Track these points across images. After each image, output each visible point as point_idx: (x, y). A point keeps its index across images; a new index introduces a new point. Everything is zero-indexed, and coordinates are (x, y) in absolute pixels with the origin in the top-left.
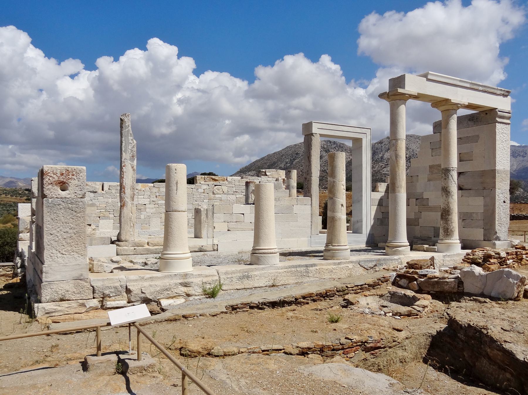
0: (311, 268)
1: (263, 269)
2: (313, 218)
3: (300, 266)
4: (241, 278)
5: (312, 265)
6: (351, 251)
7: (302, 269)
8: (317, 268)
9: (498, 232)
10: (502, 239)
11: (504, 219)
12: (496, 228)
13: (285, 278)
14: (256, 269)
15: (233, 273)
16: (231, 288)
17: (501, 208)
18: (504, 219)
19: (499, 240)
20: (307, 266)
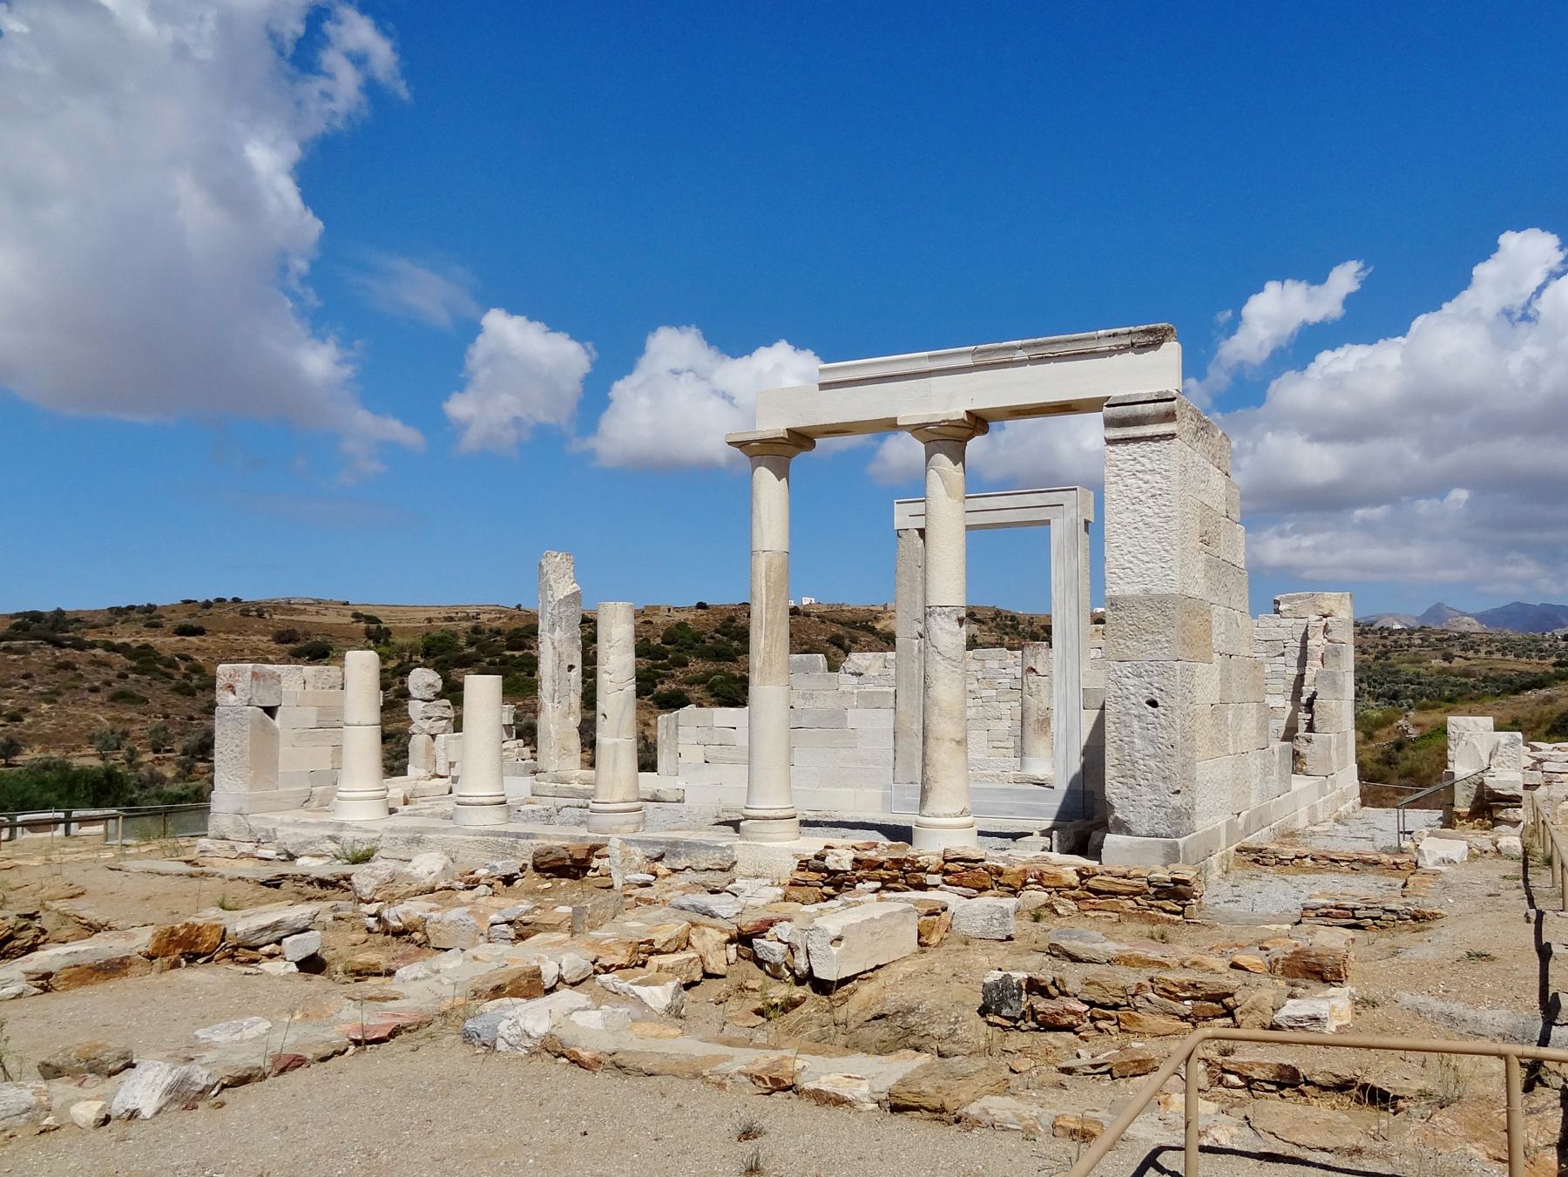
0: (522, 841)
1: (445, 831)
2: (900, 742)
3: (506, 834)
4: (409, 842)
5: (528, 836)
6: (981, 833)
7: (506, 840)
8: (534, 842)
9: (1116, 802)
10: (1133, 828)
11: (1152, 763)
12: (1108, 791)
13: (473, 853)
14: (435, 830)
15: (401, 831)
16: (392, 855)
17: (1136, 725)
18: (1152, 763)
19: (1129, 832)
20: (518, 836)
